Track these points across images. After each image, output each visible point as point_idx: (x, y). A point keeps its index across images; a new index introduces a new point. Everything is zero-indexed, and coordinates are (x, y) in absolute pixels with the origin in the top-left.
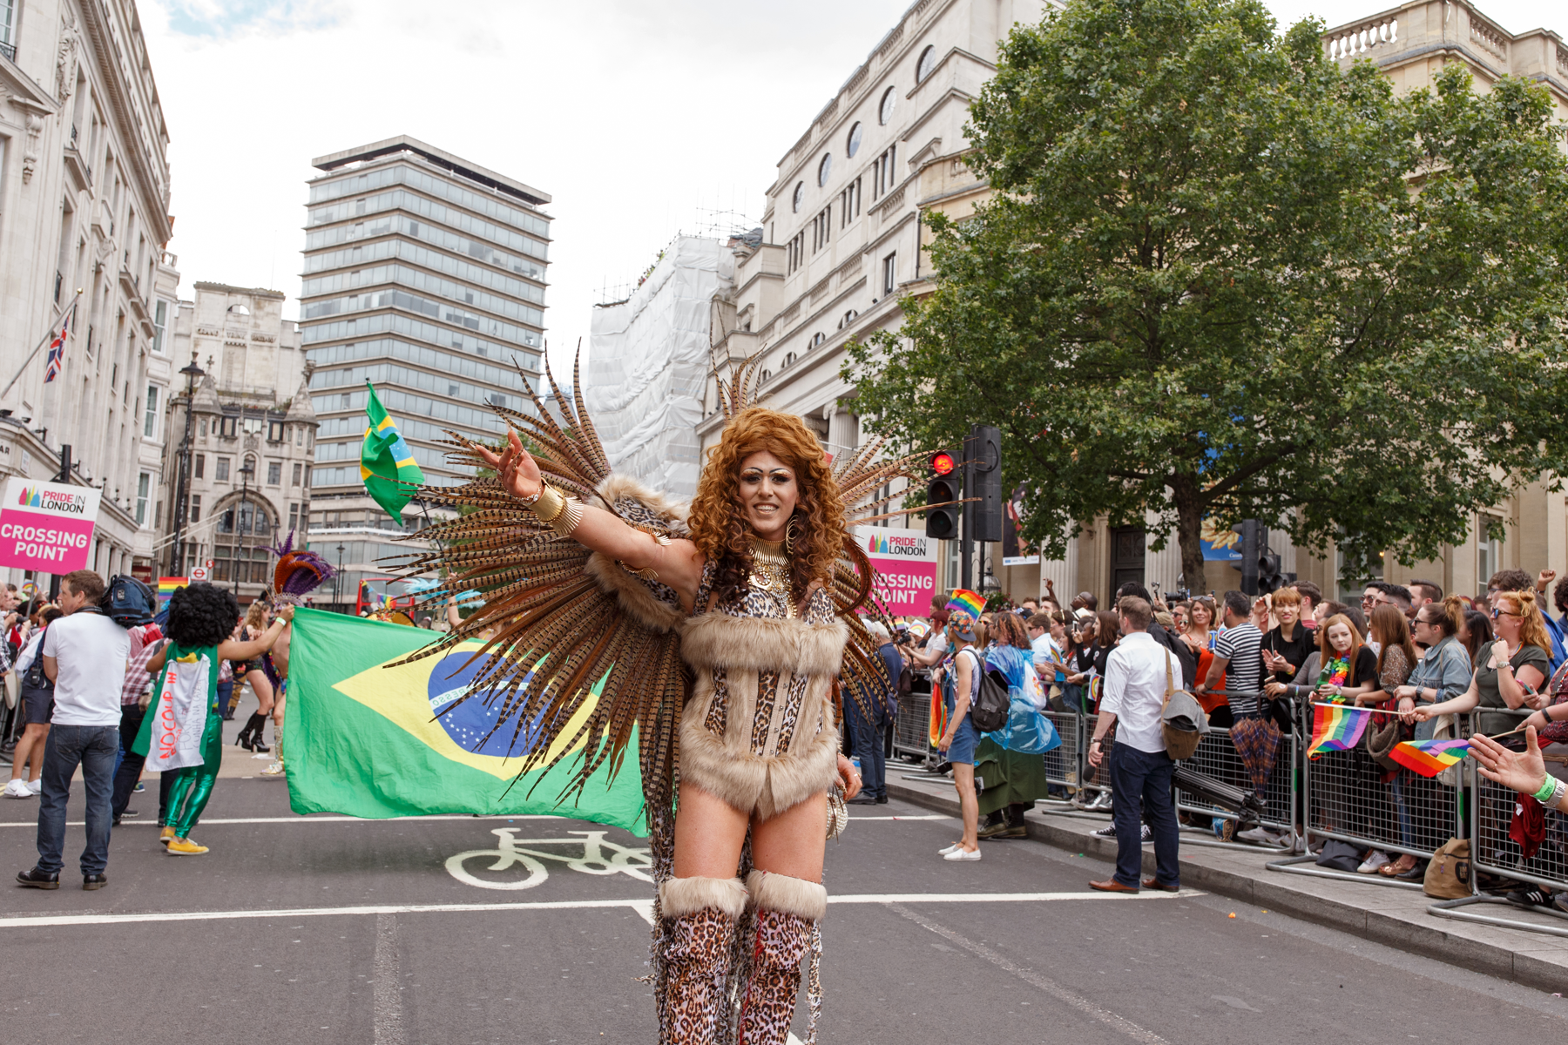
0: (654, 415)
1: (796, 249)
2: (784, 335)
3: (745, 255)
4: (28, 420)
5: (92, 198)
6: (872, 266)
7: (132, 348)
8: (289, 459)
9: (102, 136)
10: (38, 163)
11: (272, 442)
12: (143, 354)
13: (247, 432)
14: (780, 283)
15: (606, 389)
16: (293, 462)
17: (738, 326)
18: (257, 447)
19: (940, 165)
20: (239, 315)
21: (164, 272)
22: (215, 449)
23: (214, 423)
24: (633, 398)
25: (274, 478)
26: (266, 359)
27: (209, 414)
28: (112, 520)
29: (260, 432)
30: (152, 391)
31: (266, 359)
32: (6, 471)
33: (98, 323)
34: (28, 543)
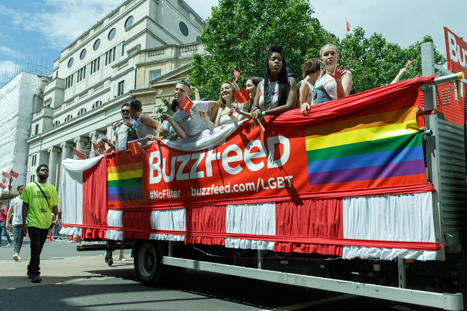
0: (7, 135)
1: (69, 81)
2: (67, 108)
3: (46, 81)
6: (114, 85)
17: (44, 105)
19: (145, 52)
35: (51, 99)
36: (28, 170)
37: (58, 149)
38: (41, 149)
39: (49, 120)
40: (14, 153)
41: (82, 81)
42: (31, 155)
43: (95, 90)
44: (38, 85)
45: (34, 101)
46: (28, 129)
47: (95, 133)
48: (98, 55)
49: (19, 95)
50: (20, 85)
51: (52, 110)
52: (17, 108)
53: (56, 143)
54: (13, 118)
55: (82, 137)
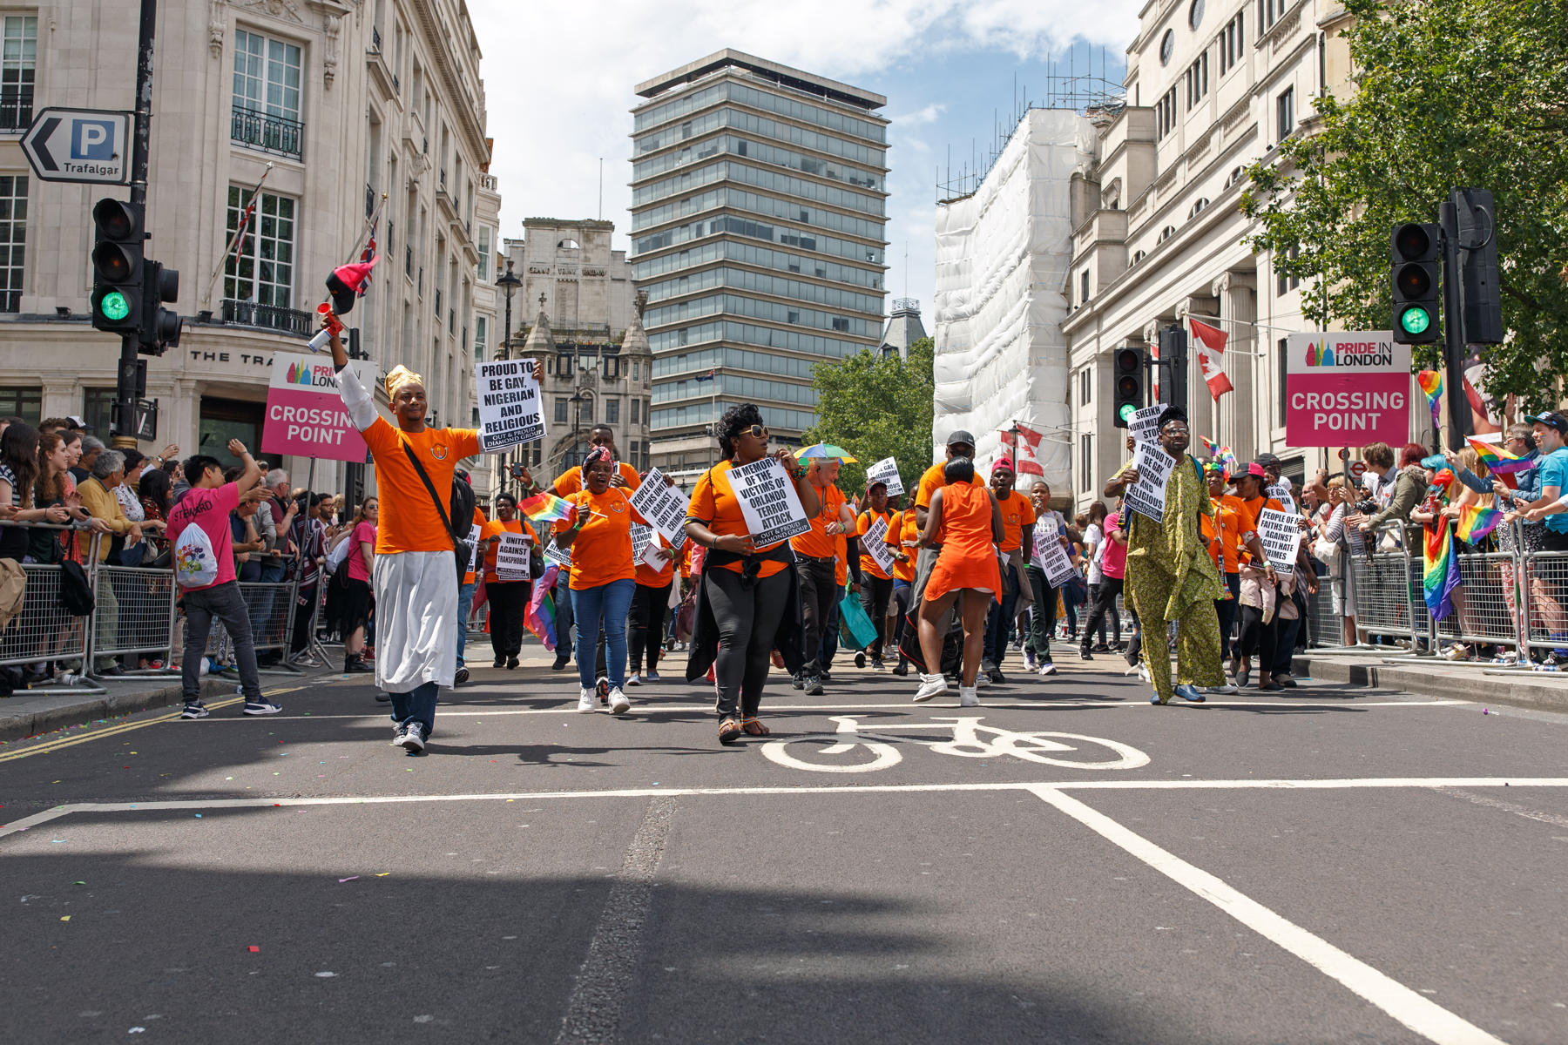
0: (1010, 315)
2: (1158, 207)
3: (1106, 124)
5: (401, 110)
6: (1264, 111)
8: (626, 395)
9: (407, 44)
10: (340, 67)
11: (607, 378)
12: (467, 283)
13: (582, 369)
14: (1148, 148)
16: (630, 397)
17: (1103, 205)
18: (593, 385)
20: (570, 250)
22: (553, 390)
23: (550, 362)
26: (598, 294)
29: (595, 369)
30: (482, 321)
31: (598, 294)
33: (416, 246)
34: (301, 426)
35: (1118, 180)
36: (1074, 420)
38: (1099, 348)
39: (1114, 253)
40: (1030, 370)
41: (1200, 104)
44: (1084, 144)
45: (1072, 196)
47: (1227, 279)
48: (1236, 6)
49: (1027, 185)
50: (1026, 156)
51: (1124, 215)
52: (1026, 227)
54: (1020, 260)
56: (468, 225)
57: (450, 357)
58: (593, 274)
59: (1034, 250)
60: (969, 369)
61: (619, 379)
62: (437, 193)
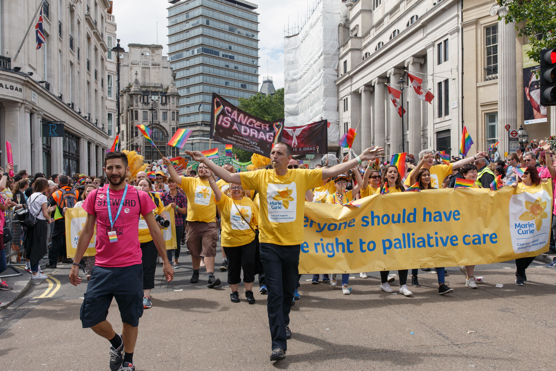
0: (315, 78)
2: (376, 34)
3: (351, 5)
4: (31, 74)
7: (96, 55)
8: (170, 110)
11: (163, 104)
13: (153, 100)
15: (291, 72)
16: (171, 111)
17: (351, 35)
18: (157, 106)
20: (146, 56)
21: (109, 23)
22: (142, 108)
23: (140, 98)
24: (305, 73)
25: (165, 119)
26: (158, 73)
27: (138, 94)
28: (95, 133)
29: (158, 100)
32: (21, 101)
33: (76, 36)
35: (358, 25)
37: (370, 87)
38: (351, 90)
39: (357, 53)
42: (341, 99)
43: (408, 1)
46: (336, 68)
47: (412, 60)
49: (322, 28)
50: (322, 17)
51: (360, 39)
52: (322, 44)
53: (366, 81)
54: (319, 57)
55: (396, 68)
56: (102, 34)
57: (96, 91)
58: (156, 65)
59: (324, 53)
60: (298, 99)
61: (167, 104)
62: (86, 15)
